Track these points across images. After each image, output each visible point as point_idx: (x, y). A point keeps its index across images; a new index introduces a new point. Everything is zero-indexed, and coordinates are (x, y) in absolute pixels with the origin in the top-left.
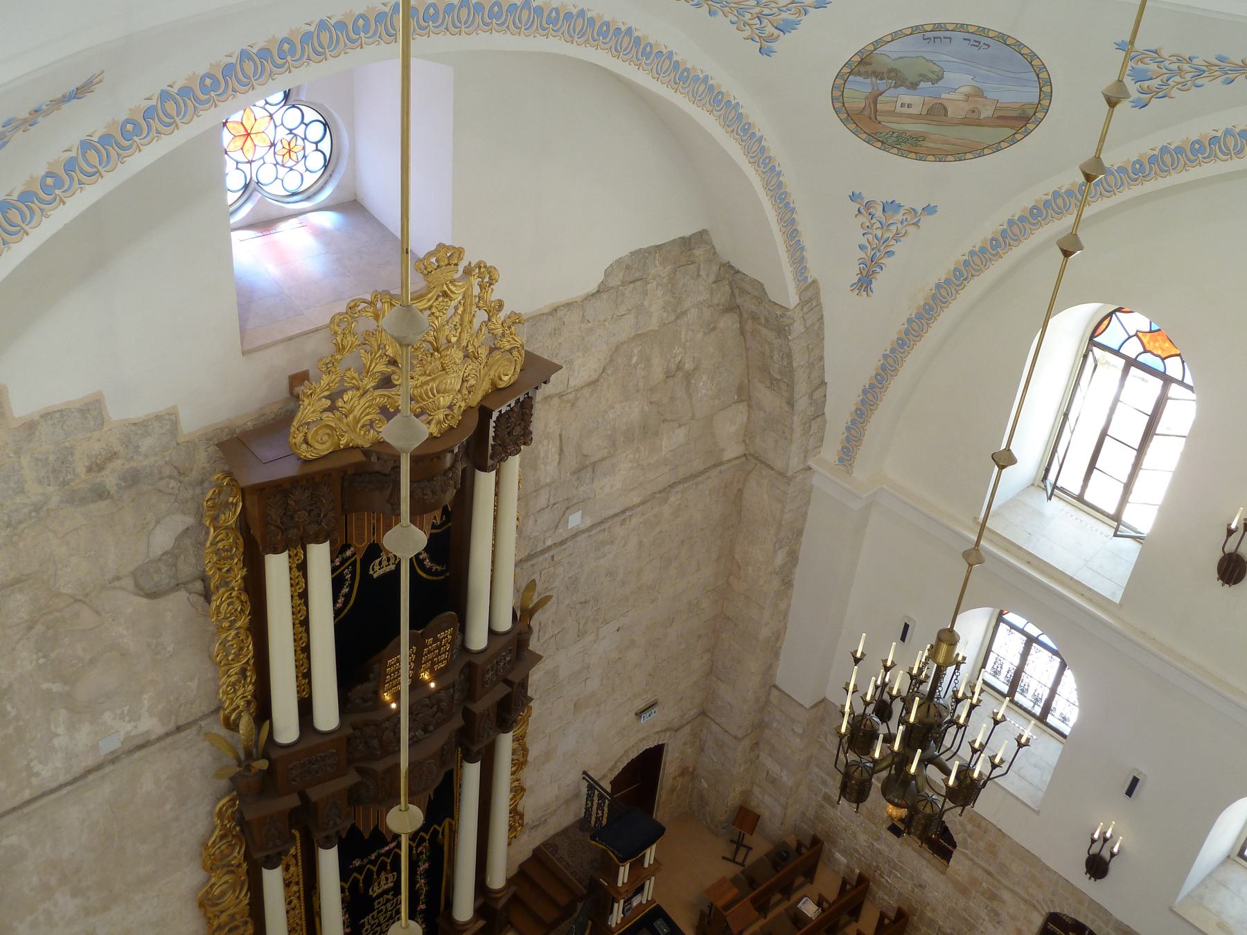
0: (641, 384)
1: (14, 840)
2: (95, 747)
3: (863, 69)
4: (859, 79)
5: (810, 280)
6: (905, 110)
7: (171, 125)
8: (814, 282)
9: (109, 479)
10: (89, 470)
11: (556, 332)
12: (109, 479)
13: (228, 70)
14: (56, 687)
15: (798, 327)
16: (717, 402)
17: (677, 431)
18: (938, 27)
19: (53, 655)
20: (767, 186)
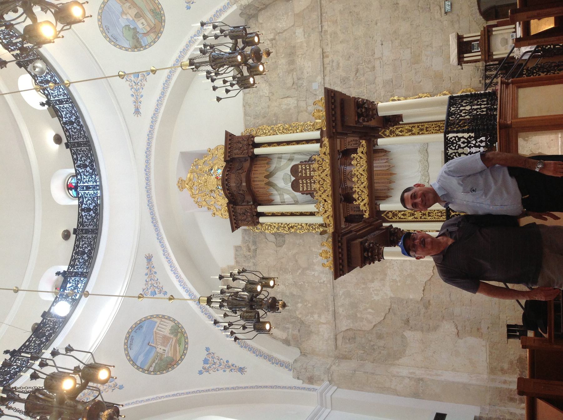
0: (274, 61)
1: (341, 292)
3: (138, 46)
4: (142, 43)
6: (145, 23)
7: (162, 238)
9: (253, 248)
10: (250, 252)
11: (250, 106)
13: (155, 226)
14: (300, 271)
16: (290, 14)
18: (110, 41)
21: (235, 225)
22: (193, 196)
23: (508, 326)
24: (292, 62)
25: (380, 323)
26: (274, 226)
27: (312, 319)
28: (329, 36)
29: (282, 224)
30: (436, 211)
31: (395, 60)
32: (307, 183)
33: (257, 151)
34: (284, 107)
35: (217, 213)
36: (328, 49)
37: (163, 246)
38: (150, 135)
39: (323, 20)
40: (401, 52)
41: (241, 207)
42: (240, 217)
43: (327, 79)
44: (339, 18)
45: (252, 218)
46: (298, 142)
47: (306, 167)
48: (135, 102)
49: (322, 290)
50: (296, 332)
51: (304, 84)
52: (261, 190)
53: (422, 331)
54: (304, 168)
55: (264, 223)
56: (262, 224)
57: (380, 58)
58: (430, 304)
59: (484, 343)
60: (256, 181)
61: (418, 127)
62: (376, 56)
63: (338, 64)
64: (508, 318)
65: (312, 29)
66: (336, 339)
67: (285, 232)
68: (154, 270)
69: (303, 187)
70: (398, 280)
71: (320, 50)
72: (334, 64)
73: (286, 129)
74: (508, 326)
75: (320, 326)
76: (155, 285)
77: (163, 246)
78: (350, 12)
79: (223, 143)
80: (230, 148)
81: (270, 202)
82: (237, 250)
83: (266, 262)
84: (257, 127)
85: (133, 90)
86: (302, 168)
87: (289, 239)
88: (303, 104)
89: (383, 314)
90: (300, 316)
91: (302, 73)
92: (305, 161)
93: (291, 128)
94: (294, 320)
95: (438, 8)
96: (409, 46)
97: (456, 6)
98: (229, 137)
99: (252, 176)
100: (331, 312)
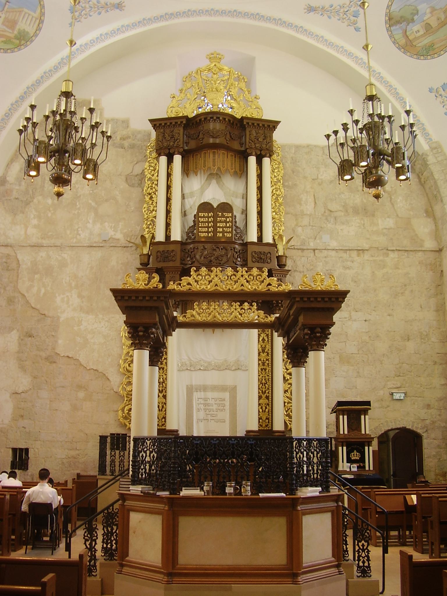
1: (65, 256)
2: (100, 235)
5: (433, 141)
8: (436, 142)
9: (126, 143)
10: (121, 139)
12: (126, 143)
14: (93, 204)
15: (431, 160)
16: (411, 213)
17: (388, 219)
19: (95, 191)
20: (389, 91)
21: (157, 123)
22: (199, 71)
23: (27, 450)
24: (356, 211)
25: (27, 302)
26: (153, 175)
27: (32, 216)
28: (381, 258)
29: (157, 185)
30: (165, 376)
31: (347, 335)
32: (208, 222)
33: (252, 160)
34: (304, 197)
35: (174, 101)
36: (366, 256)
37: (134, 25)
38: (279, 22)
39: (400, 252)
40: (354, 343)
41: (181, 133)
42: (168, 131)
43: (333, 253)
44: (400, 271)
45: (166, 148)
46: (260, 214)
47: (228, 222)
48: (323, 8)
49: (68, 232)
50: (15, 194)
51: (329, 225)
52: (201, 161)
53: (18, 352)
54: (228, 220)
55: (158, 161)
56: (157, 159)
57: (350, 318)
58: (51, 363)
59: (6, 421)
60: (214, 156)
61: (267, 360)
62: (353, 313)
63: (348, 268)
64: (36, 450)
65: (391, 239)
66: (7, 246)
67: (145, 189)
68: (103, 12)
69: (204, 217)
70: (81, 327)
71: (366, 246)
72: (349, 263)
73: (277, 199)
74: (27, 450)
75: (23, 226)
76: (84, 12)
77: (134, 25)
78: (405, 285)
79: (266, 116)
80: (258, 125)
81: (186, 171)
82: (123, 122)
83: (113, 163)
84: (282, 161)
85: (339, 7)
86: (228, 217)
87: (136, 193)
88: (305, 221)
89: (38, 307)
90: (35, 201)
91: (343, 224)
92: (236, 222)
93: (278, 205)
94: (31, 193)
95: (399, 385)
96: (361, 352)
97: (398, 404)
98: (272, 125)
99: (221, 152)
100: (40, 241)
